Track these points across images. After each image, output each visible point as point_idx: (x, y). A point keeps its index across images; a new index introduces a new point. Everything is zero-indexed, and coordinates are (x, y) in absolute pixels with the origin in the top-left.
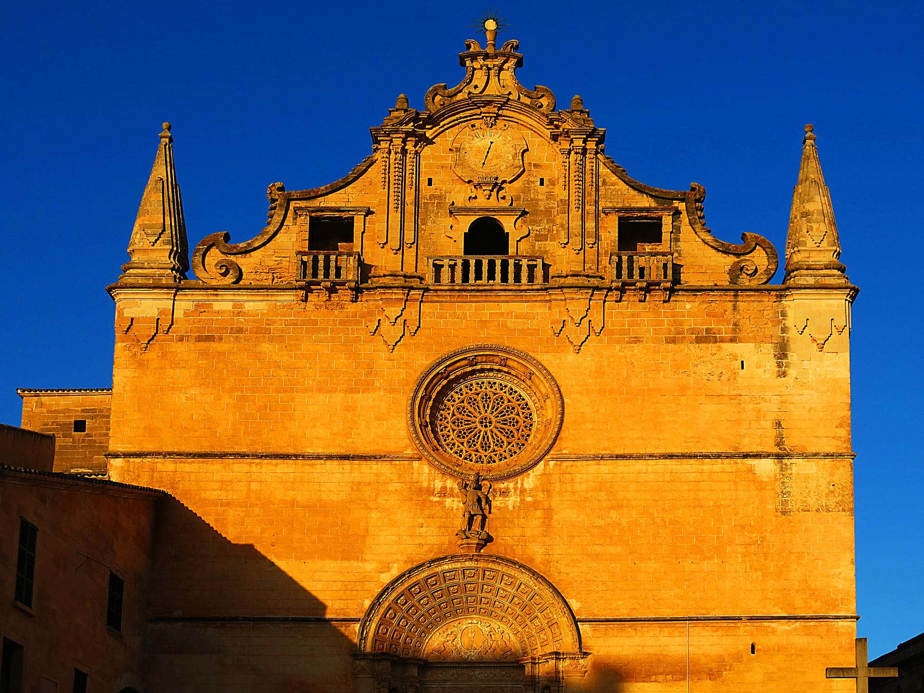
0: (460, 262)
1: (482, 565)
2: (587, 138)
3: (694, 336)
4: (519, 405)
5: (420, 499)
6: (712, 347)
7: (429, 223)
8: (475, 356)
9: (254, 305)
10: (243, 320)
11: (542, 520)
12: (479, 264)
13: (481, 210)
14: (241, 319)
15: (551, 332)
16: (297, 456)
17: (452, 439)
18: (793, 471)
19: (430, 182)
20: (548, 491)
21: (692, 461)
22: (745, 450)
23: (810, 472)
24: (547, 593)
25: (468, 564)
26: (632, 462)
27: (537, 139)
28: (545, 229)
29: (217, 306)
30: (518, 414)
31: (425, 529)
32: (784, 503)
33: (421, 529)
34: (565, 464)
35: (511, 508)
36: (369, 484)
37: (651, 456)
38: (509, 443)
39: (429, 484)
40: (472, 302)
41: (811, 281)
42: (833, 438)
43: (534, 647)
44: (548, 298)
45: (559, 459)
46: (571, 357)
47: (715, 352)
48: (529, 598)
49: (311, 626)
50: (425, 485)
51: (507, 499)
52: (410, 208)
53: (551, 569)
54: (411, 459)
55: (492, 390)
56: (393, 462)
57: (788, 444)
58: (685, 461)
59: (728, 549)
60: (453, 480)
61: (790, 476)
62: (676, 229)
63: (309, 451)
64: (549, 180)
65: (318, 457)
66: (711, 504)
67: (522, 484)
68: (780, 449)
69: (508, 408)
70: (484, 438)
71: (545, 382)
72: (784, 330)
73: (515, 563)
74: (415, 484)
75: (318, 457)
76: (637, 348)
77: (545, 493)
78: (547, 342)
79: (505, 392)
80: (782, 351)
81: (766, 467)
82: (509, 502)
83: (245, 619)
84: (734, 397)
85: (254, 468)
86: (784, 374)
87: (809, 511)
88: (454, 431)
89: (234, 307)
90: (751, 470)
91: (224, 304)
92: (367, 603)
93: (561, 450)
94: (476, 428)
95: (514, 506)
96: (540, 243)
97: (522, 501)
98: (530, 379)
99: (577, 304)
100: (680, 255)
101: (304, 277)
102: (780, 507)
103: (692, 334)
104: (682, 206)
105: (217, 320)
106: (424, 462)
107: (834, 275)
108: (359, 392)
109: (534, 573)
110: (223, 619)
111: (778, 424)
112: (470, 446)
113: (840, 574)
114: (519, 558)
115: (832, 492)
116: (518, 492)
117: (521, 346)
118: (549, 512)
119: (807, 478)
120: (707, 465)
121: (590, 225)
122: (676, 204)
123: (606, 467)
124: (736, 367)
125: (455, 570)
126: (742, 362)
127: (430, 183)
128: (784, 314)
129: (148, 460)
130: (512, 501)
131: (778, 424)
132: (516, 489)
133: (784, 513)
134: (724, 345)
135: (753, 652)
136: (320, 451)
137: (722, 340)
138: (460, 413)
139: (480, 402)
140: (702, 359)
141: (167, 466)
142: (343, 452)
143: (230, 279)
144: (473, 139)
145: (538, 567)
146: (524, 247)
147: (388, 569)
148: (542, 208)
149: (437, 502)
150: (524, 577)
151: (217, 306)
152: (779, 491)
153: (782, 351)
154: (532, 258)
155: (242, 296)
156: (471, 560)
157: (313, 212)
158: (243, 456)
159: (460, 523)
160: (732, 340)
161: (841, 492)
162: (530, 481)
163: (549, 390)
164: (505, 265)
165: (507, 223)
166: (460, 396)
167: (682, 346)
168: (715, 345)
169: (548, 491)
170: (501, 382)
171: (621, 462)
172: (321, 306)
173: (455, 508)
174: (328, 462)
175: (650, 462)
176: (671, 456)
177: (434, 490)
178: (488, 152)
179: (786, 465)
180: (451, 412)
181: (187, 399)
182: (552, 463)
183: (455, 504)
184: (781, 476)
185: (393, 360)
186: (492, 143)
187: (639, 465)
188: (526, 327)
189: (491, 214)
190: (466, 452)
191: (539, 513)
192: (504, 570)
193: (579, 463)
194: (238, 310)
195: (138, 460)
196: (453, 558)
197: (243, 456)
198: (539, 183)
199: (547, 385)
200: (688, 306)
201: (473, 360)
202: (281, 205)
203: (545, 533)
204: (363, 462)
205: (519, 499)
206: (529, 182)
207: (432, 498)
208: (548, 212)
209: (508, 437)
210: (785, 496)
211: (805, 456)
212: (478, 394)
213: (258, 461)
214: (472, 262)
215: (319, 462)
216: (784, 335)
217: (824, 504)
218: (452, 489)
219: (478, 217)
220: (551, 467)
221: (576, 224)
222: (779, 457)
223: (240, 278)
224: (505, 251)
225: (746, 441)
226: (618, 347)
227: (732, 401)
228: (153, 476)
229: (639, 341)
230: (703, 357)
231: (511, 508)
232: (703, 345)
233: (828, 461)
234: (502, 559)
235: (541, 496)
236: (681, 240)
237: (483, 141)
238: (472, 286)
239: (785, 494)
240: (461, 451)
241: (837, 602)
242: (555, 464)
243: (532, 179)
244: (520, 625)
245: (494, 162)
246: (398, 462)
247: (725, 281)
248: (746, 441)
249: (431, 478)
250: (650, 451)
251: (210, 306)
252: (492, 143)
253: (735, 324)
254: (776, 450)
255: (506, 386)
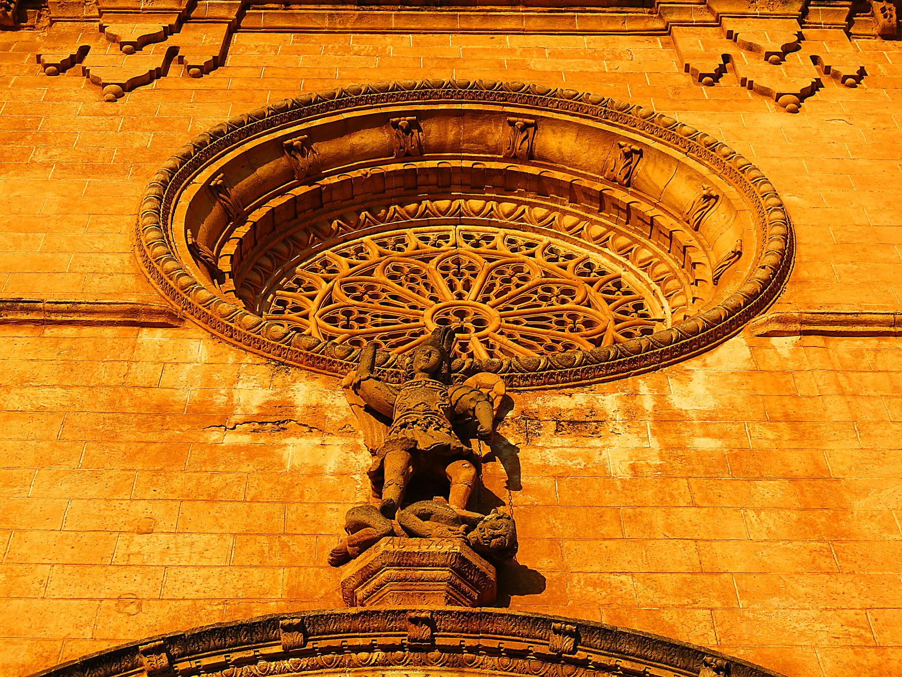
8: (419, 114)
11: (795, 516)
20: (793, 421)
31: (161, 540)
33: (138, 538)
34: (843, 346)
44: (659, 25)
56: (49, 332)
60: (324, 382)
95: (633, 467)
98: (628, 183)
149: (237, 449)
169: (793, 421)
182: (784, 345)
201: (408, 130)
203: (824, 563)
207: (214, 436)
242: (796, 345)
246: (69, 331)
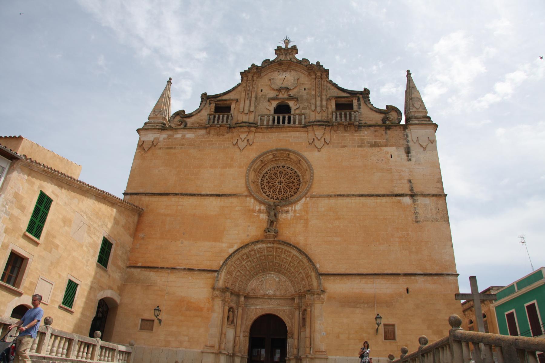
0: (271, 118)
1: (275, 245)
2: (322, 73)
3: (369, 144)
4: (295, 175)
5: (249, 214)
6: (378, 149)
7: (260, 104)
9: (190, 135)
10: (184, 141)
11: (303, 225)
12: (279, 118)
13: (281, 99)
14: (184, 140)
15: (308, 143)
16: (198, 195)
17: (266, 190)
18: (419, 203)
19: (262, 91)
21: (372, 198)
22: (396, 193)
23: (426, 203)
24: (305, 260)
25: (269, 245)
26: (344, 198)
27: (303, 75)
28: (306, 105)
29: (176, 136)
30: (294, 179)
31: (250, 228)
32: (416, 217)
34: (314, 199)
35: (289, 218)
36: (227, 207)
37: (353, 195)
38: (290, 192)
39: (254, 207)
40: (276, 132)
41: (417, 122)
42: (436, 187)
43: (300, 289)
45: (312, 197)
46: (316, 154)
47: (379, 151)
48: (297, 263)
49: (195, 273)
50: (252, 208)
51: (288, 215)
52: (253, 99)
53: (308, 248)
54: (246, 196)
55: (284, 169)
56: (239, 198)
57: (415, 190)
58: (368, 198)
59: (392, 240)
61: (418, 205)
62: (359, 104)
63: (204, 193)
64: (308, 89)
65: (207, 195)
66: (382, 218)
67: (295, 208)
68: (412, 192)
69: (290, 176)
70: (279, 189)
71: (305, 163)
72: (408, 142)
73: (290, 245)
74: (247, 208)
75: (207, 195)
76: (346, 149)
77: (305, 212)
78: (307, 147)
79: (289, 170)
80: (408, 151)
81: (407, 200)
82: (289, 216)
83: (167, 268)
84: (389, 170)
85: (181, 200)
86: (410, 160)
87: (428, 221)
88: (266, 186)
89: (182, 136)
90: (399, 202)
91: (178, 135)
92: (222, 262)
93: (313, 193)
94: (276, 185)
96: (304, 110)
97: (295, 215)
98: (299, 163)
99: (319, 132)
100: (361, 114)
101: (208, 123)
102: (414, 219)
103: (369, 143)
104: (361, 96)
105: (175, 141)
106: (252, 198)
107: (427, 120)
108: (227, 168)
109: (299, 250)
110: (158, 268)
111: (410, 181)
112: (273, 193)
113: (447, 252)
114: (292, 242)
115: (438, 212)
116: (293, 212)
117: (296, 149)
118: (307, 221)
119: (425, 205)
120: (379, 200)
121: (324, 103)
122: (358, 95)
123: (332, 201)
124: (389, 157)
125: (263, 248)
126: (391, 155)
127: (262, 91)
128: (407, 135)
129: (139, 196)
130: (290, 215)
131: (410, 181)
132: (292, 210)
133: (417, 222)
134: (383, 148)
135: (408, 293)
136: (208, 193)
137: (382, 146)
138: (270, 179)
139: (278, 174)
140: (374, 154)
141: (146, 199)
142: (218, 193)
143: (182, 126)
144: (279, 76)
145: (301, 246)
146: (298, 112)
147: (233, 246)
148: (305, 98)
150: (294, 252)
151: (176, 136)
152: (413, 211)
153: (408, 151)
154: (300, 115)
155: (185, 132)
156: (270, 243)
157: (216, 101)
158: (176, 194)
159: (265, 225)
160: (386, 146)
161: (442, 212)
162: (298, 207)
163: (307, 167)
164: (289, 118)
165: (291, 104)
166: (270, 172)
167: (365, 148)
168: (379, 148)
170: (288, 166)
171: (339, 198)
172: (215, 135)
173: (264, 218)
174: (211, 198)
175: (353, 198)
176: (362, 196)
177: (255, 211)
178: (284, 80)
179: (415, 199)
180: (266, 178)
181: (159, 171)
183: (264, 216)
184: (414, 205)
185: (242, 155)
186: (286, 76)
187: (348, 200)
188: (298, 141)
189: (285, 100)
190: (271, 195)
191: (302, 221)
192: (285, 248)
193: (320, 199)
194: (183, 137)
195: (135, 196)
196: (262, 242)
197: (176, 194)
198: (304, 90)
199: (306, 165)
200: (366, 133)
202: (205, 100)
204: (226, 198)
205: (293, 215)
206: (300, 89)
207: (254, 214)
208: (307, 99)
209: (290, 189)
210: (416, 214)
211: (425, 195)
212: (277, 171)
213: (182, 197)
214: (276, 117)
215: (207, 197)
216: (408, 144)
217: (435, 218)
218: (263, 210)
219: (279, 102)
220: (308, 200)
221: (318, 103)
222: (412, 196)
223: (185, 126)
224: (290, 113)
225: (396, 189)
226: (337, 149)
227: (388, 171)
228: (140, 203)
229: (346, 146)
230: (374, 153)
231: (289, 218)
232: (374, 148)
233: (434, 199)
234: (285, 243)
235: (303, 213)
236: (361, 108)
237: (282, 76)
238: (276, 125)
239: (416, 213)
240: (269, 195)
241: (447, 266)
243: (301, 88)
244: (293, 278)
245: (287, 83)
246: (240, 198)
247: (380, 123)
248: (396, 189)
249: (254, 205)
250: (352, 193)
251: (173, 136)
252: (286, 76)
253: (387, 140)
254: (410, 193)
255: (289, 168)
